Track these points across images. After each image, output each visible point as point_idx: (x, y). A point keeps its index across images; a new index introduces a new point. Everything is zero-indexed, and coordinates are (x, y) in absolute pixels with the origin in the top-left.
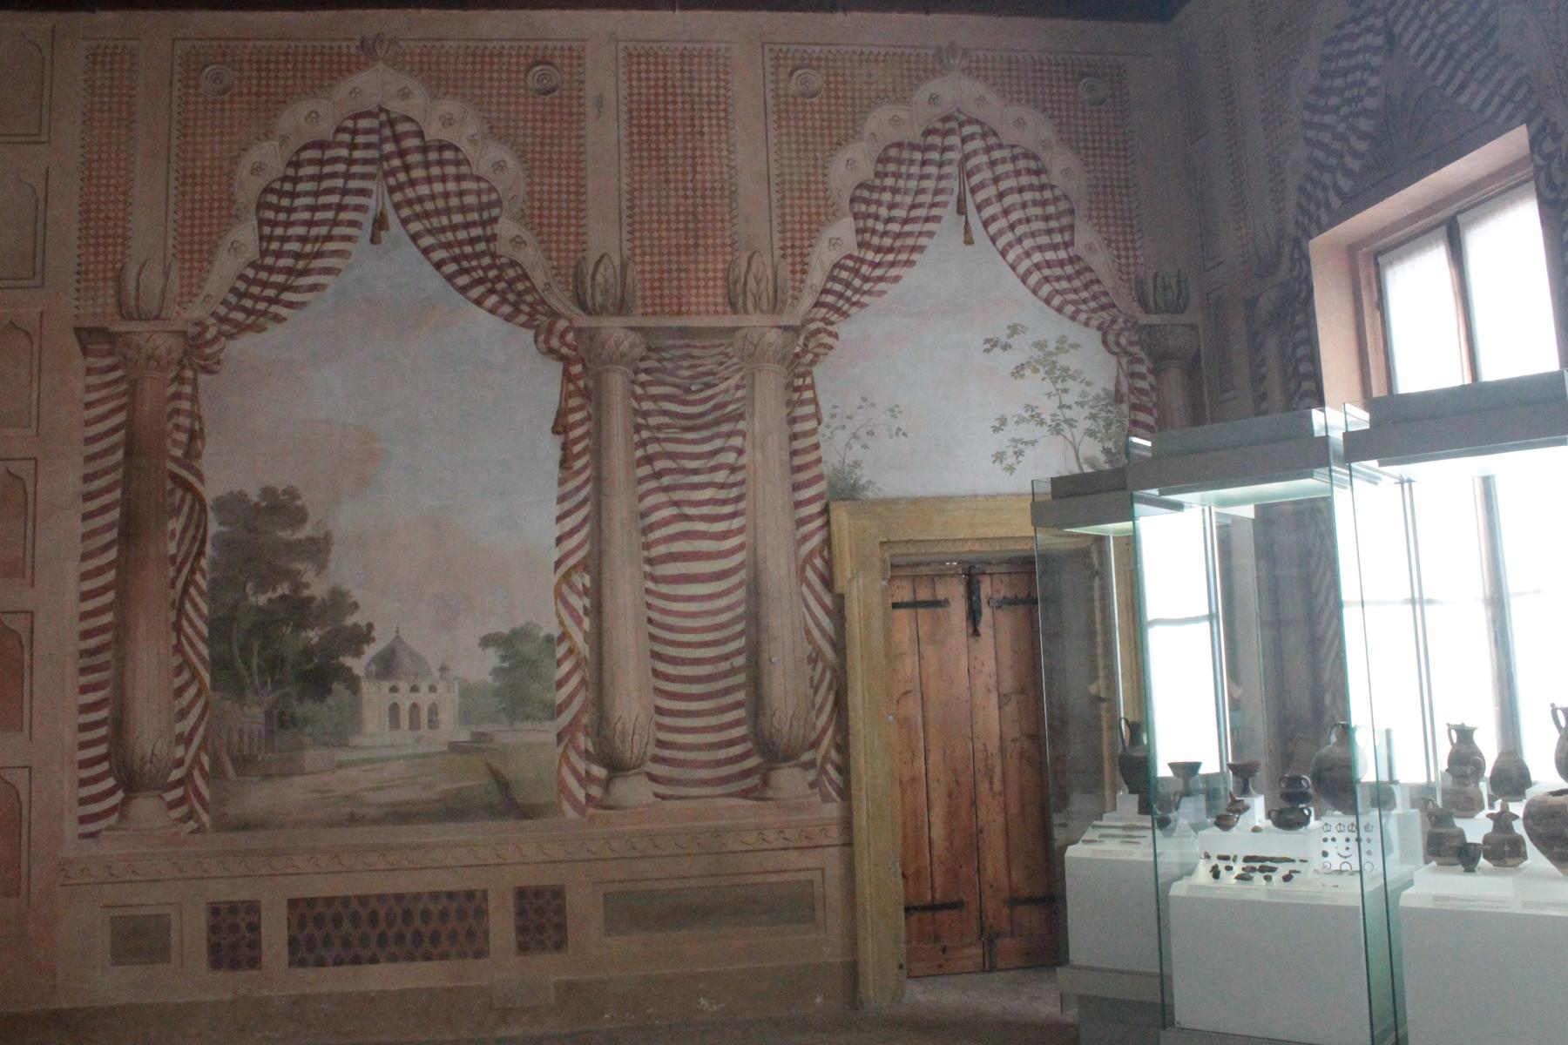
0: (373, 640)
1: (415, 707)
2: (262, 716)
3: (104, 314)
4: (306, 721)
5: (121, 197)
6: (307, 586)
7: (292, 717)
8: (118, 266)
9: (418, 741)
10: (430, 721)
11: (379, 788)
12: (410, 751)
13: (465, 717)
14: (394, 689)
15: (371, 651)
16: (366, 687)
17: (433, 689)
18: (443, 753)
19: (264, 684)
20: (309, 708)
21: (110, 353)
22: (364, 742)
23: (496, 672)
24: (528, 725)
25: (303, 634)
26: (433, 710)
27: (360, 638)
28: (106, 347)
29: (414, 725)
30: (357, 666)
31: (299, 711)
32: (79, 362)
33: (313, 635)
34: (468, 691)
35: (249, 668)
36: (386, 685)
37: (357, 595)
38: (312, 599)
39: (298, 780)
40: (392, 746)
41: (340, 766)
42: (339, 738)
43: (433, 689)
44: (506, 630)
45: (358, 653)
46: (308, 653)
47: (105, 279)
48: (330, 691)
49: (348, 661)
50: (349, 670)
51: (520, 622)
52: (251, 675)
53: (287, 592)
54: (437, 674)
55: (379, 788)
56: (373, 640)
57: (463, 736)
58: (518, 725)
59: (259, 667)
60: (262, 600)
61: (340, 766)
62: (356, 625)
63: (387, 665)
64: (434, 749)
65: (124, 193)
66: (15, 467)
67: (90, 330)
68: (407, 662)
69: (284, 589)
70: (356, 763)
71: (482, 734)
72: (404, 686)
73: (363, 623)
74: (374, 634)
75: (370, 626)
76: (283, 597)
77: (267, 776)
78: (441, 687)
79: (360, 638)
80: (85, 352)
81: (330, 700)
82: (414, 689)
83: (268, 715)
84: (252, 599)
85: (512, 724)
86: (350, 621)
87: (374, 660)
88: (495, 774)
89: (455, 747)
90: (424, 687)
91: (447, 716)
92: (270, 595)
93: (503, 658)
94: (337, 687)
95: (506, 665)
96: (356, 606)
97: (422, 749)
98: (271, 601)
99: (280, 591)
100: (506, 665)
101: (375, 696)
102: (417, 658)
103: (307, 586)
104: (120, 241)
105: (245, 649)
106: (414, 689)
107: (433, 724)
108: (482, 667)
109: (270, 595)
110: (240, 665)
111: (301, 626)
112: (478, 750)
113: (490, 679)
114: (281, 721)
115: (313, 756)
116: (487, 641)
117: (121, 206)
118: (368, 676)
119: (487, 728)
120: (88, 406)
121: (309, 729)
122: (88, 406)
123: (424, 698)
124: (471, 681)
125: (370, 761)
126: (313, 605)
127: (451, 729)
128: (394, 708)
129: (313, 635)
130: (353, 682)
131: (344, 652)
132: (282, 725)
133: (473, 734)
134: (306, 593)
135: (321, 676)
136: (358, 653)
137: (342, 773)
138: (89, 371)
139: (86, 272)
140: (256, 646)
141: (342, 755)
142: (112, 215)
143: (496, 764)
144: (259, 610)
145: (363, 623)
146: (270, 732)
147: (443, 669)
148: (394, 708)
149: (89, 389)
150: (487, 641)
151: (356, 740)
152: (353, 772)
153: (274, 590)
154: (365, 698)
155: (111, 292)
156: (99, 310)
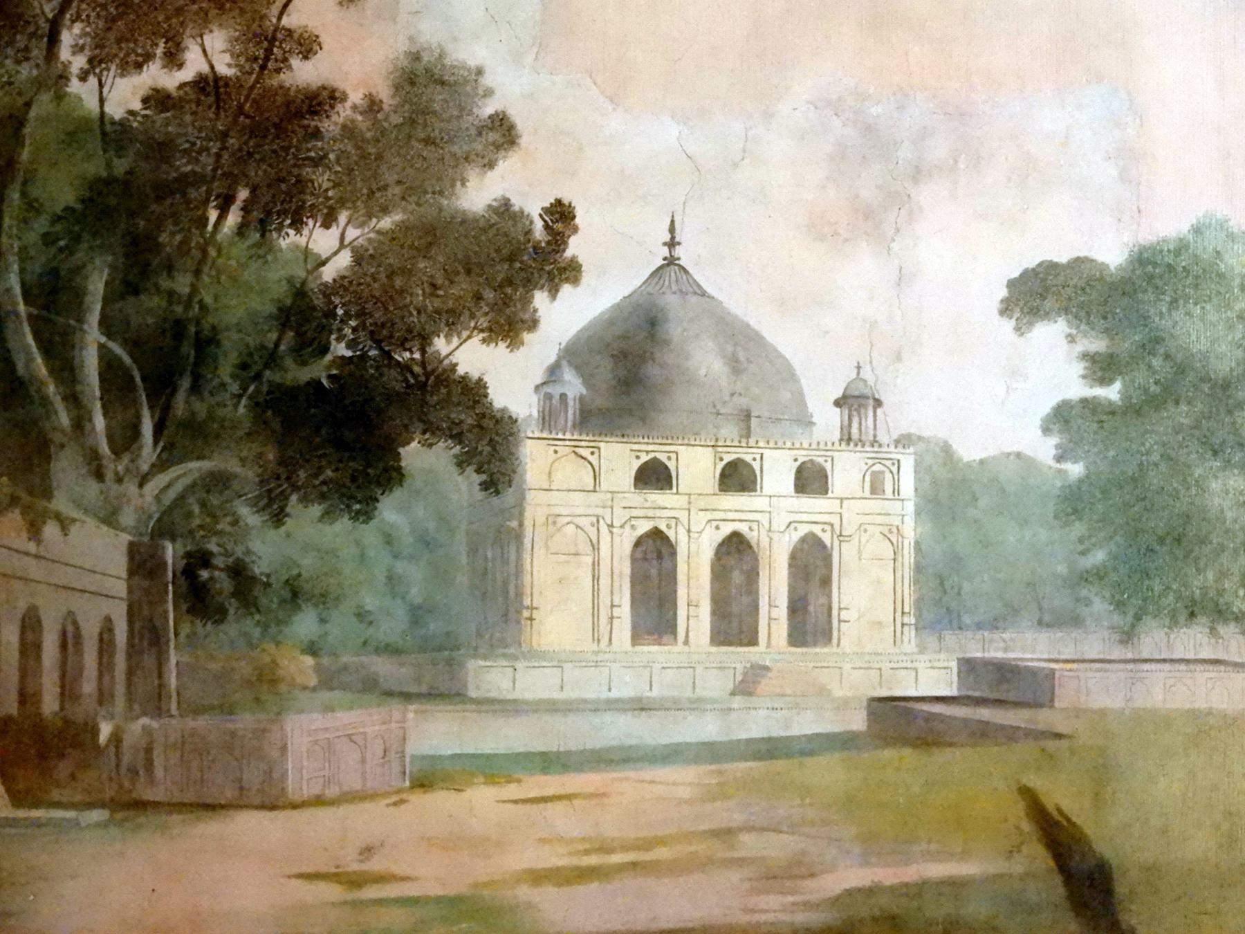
0: (571, 272)
1: (735, 549)
2: (119, 564)
4: (295, 594)
6: (308, 46)
7: (238, 571)
9: (747, 685)
10: (797, 608)
11: (582, 875)
12: (707, 729)
13: (940, 598)
14: (654, 476)
15: (563, 316)
16: (537, 459)
17: (810, 480)
18: (844, 742)
19: (125, 439)
20: (306, 538)
22: (532, 683)
23: (1063, 417)
24: (1193, 640)
25: (289, 240)
26: (813, 564)
27: (526, 258)
29: (733, 624)
30: (508, 374)
31: (267, 547)
33: (327, 248)
34: (953, 491)
35: (66, 370)
36: (620, 458)
37: (508, 87)
38: (320, 101)
39: (250, 826)
40: (640, 706)
41: (427, 778)
42: (432, 664)
43: (810, 480)
44: (1112, 254)
45: (509, 326)
46: (304, 316)
48: (392, 476)
49: (470, 355)
50: (473, 391)
51: (1167, 224)
52: (74, 399)
53: (224, 68)
54: (828, 420)
55: (582, 875)
56: (571, 272)
57: (931, 676)
58: (1153, 639)
59: (109, 365)
60: (124, 95)
61: (427, 778)
62: (504, 209)
63: (627, 376)
64: (806, 724)
68: (705, 360)
69: (212, 52)
70: (493, 768)
71: (1004, 672)
72: (696, 465)
73: (533, 206)
74: (575, 247)
75: (561, 214)
76: (208, 85)
77: (130, 807)
78: (847, 472)
79: (526, 258)
81: (389, 509)
82: (736, 477)
83: (143, 563)
84: (83, 92)
85: (1128, 636)
86: (477, 194)
87: (576, 354)
88: (1057, 836)
89: (897, 720)
90: (777, 473)
91: (868, 593)
92: (156, 76)
93: (1102, 367)
94: (417, 455)
95: (1112, 392)
96: (503, 132)
97: (758, 723)
98: (157, 99)
99: (194, 64)
100: (1112, 392)
101: (573, 495)
102: (743, 345)
103: (308, 46)
105: (53, 296)
106: (736, 477)
107: (810, 623)
108: (1010, 397)
109: (156, 76)
110: (32, 361)
111: (286, 203)
112: (983, 733)
113: (1044, 449)
114: (195, 585)
115: (316, 734)
116: (1039, 293)
118: (548, 418)
119: (1028, 647)
121: (305, 624)
123: (776, 516)
124: (969, 451)
125: (549, 762)
126: (330, 125)
127: (881, 647)
128: (655, 550)
129: (327, 248)
130: (486, 443)
131: (452, 320)
132: (199, 600)
133: (969, 667)
134: (303, 74)
135: (358, 410)
136: (509, 326)
137: (440, 801)
140: (96, 285)
141: (437, 734)
143: (1063, 796)
144: (114, 135)
145: (533, 206)
146: (147, 636)
147: (854, 401)
148: (655, 550)
150: (1039, 293)
151: (490, 677)
152: (482, 803)
153: (173, 59)
154: (536, 508)
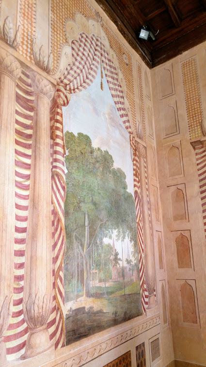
3: (198, 136)
5: (198, 101)
8: (200, 121)
21: (202, 148)
28: (201, 146)
32: (193, 152)
47: (197, 126)
65: (198, 100)
66: (179, 187)
67: (195, 142)
80: (194, 149)
104: (199, 114)
117: (198, 104)
120: (198, 164)
122: (198, 164)
138: (197, 154)
139: (191, 126)
142: (196, 107)
149: (197, 160)
155: (199, 129)
156: (197, 135)
